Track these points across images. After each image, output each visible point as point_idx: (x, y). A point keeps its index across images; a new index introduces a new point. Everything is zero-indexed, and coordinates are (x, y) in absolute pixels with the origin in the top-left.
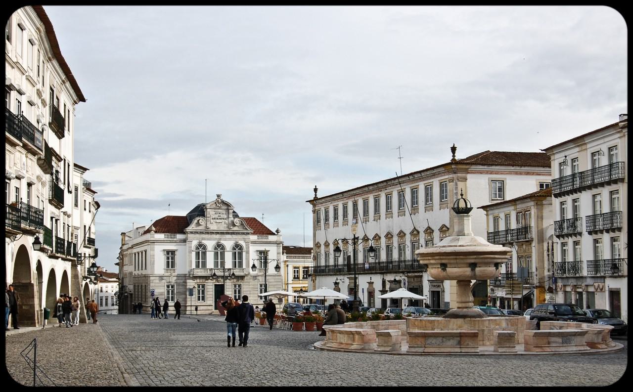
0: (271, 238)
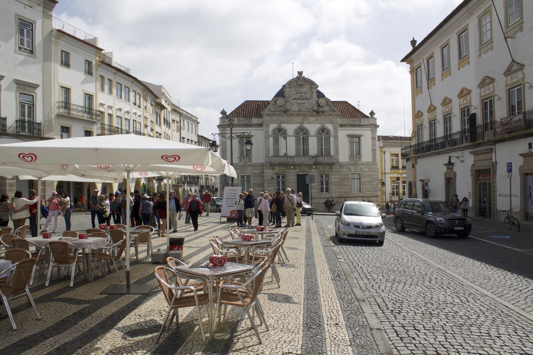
0: (364, 121)
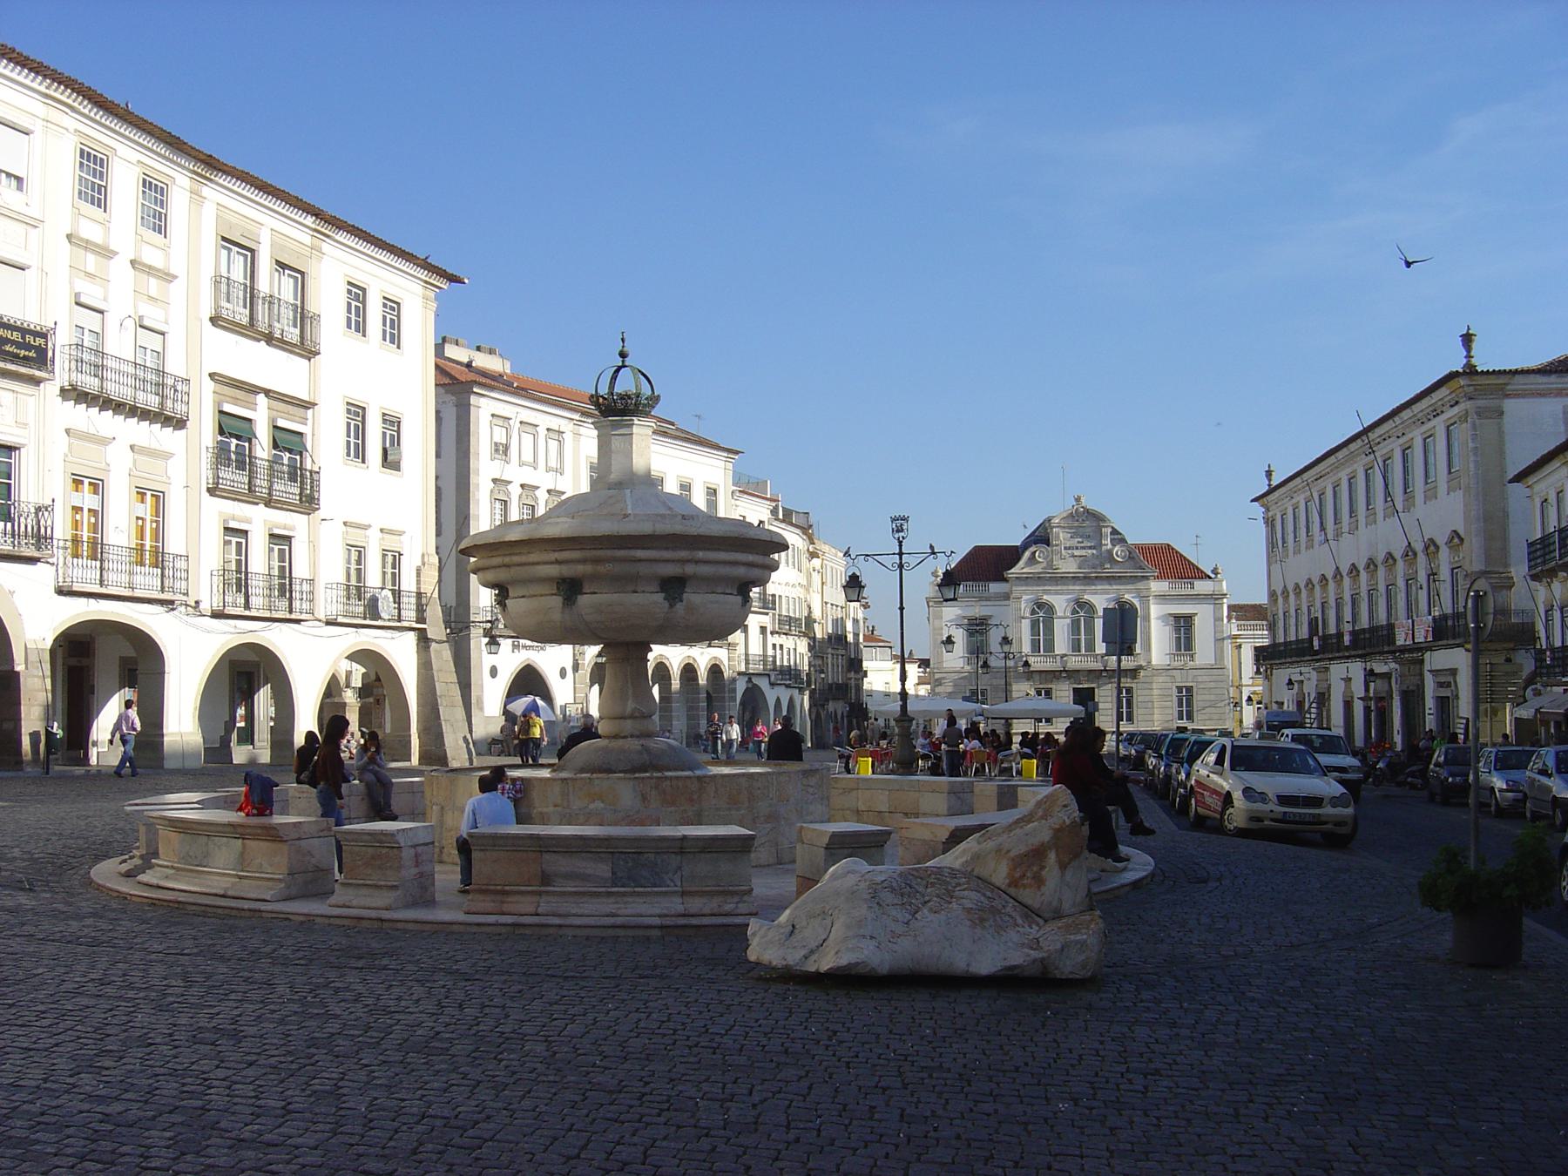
0: (1201, 586)
